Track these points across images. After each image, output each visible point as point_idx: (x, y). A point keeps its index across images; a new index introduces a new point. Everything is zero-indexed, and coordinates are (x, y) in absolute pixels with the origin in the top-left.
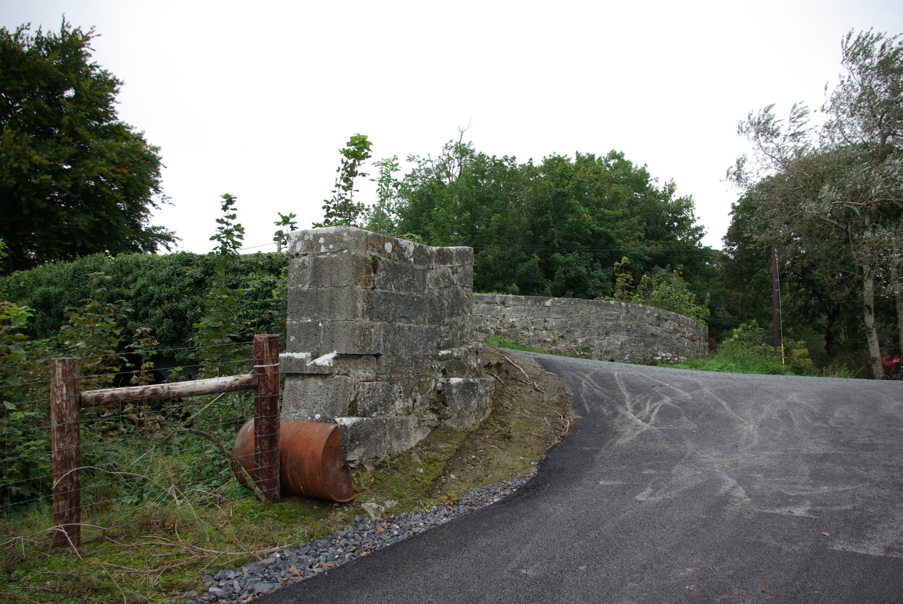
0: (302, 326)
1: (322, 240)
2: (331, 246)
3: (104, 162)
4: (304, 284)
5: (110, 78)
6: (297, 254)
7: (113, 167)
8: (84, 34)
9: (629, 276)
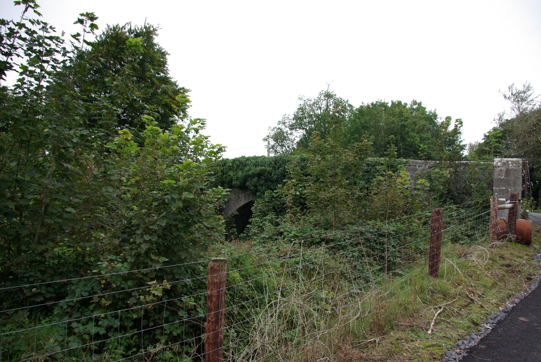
0: (500, 190)
1: (510, 163)
2: (514, 165)
3: (167, 96)
4: (502, 176)
5: (163, 51)
6: (498, 167)
7: (171, 100)
8: (154, 28)
9: (452, 169)
